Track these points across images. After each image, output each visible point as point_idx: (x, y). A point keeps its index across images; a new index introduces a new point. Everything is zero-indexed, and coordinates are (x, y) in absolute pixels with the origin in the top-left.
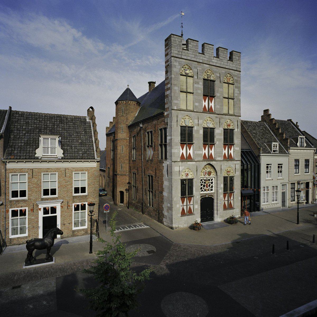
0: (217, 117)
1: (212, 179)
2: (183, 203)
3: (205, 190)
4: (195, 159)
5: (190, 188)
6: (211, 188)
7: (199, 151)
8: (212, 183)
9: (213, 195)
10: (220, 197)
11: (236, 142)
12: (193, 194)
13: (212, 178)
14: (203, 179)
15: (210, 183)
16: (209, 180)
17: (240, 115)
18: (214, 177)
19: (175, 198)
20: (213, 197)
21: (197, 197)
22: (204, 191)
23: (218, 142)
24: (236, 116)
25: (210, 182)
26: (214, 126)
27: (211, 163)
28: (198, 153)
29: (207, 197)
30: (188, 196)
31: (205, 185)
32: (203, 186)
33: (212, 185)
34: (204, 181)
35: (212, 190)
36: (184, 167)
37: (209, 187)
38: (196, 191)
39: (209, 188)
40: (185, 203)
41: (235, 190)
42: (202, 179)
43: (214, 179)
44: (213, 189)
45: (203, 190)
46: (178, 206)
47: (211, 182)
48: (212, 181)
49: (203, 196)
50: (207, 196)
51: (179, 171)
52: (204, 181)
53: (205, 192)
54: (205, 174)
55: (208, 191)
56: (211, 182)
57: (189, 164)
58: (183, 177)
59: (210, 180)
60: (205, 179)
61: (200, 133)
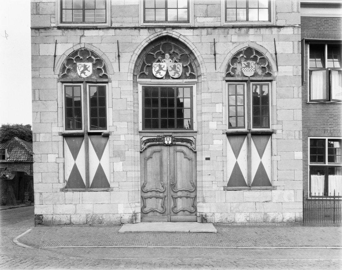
9: (191, 138)
10: (212, 144)
27: (175, 34)
46: (52, 158)
51: (55, 56)
54: (158, 72)
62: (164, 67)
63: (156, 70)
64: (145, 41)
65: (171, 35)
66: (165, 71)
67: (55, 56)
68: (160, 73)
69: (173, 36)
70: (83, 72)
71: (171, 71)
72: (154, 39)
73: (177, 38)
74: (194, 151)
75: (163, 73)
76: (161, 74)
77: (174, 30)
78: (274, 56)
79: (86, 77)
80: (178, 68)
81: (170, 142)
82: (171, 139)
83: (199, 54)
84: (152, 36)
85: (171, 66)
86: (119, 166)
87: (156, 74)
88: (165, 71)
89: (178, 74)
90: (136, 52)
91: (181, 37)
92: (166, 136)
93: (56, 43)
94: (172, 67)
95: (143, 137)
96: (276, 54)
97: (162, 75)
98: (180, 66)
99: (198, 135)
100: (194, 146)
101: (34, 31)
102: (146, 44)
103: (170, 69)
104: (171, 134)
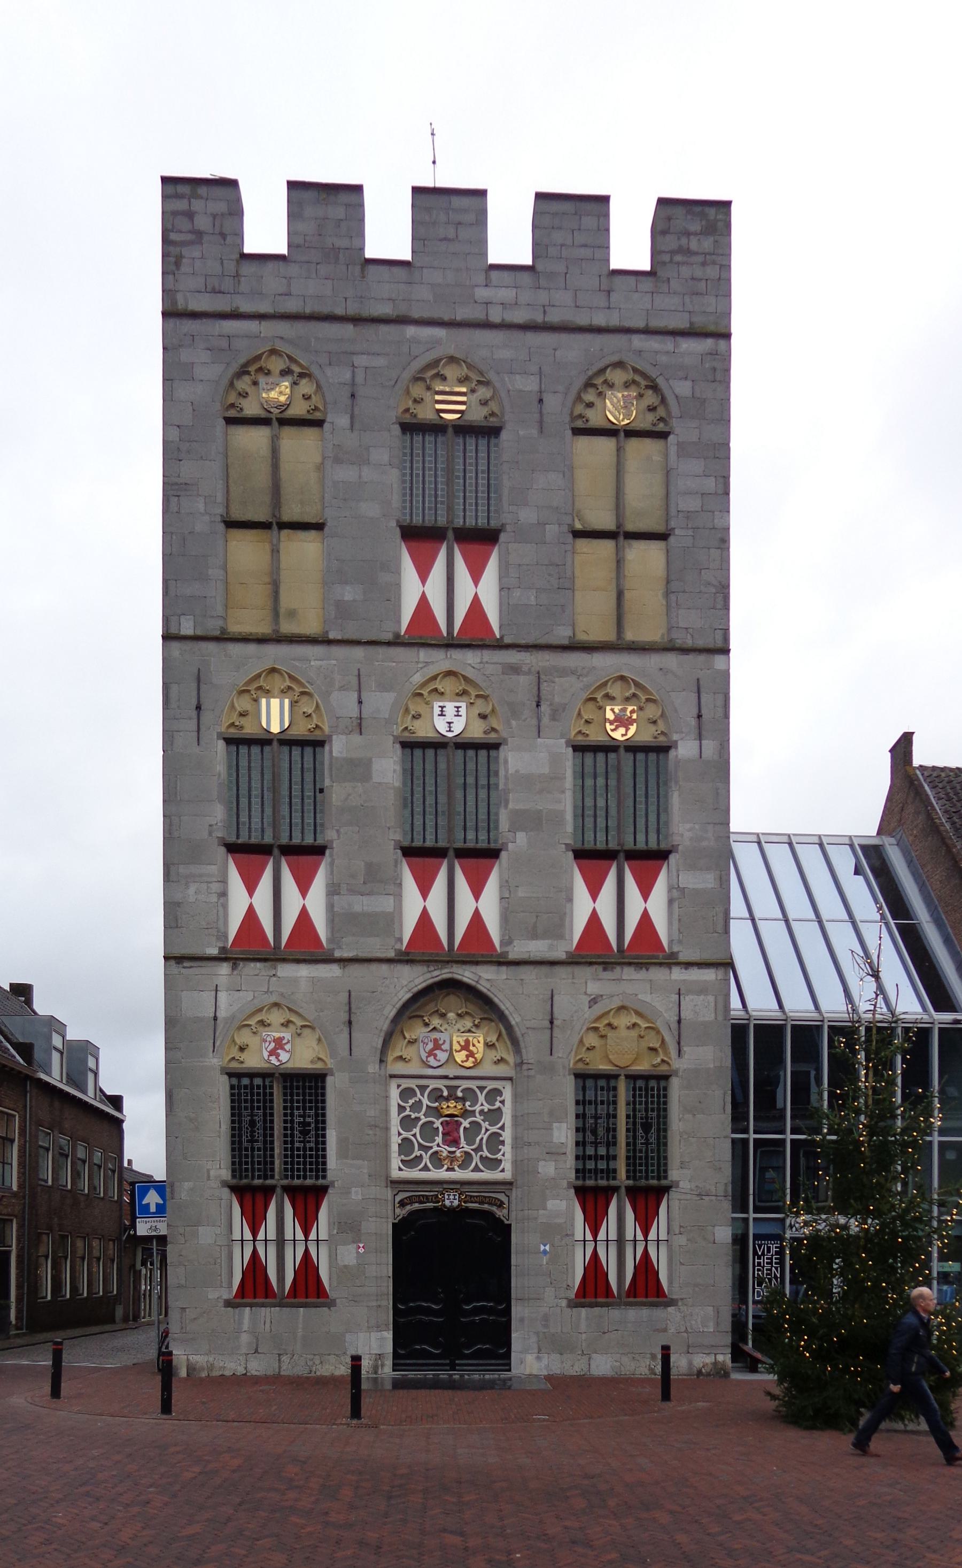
0: (515, 669)
1: (497, 1092)
2: (255, 1221)
3: (437, 1160)
4: (340, 948)
5: (305, 1133)
6: (486, 1153)
7: (370, 894)
8: (494, 1115)
9: (502, 1197)
11: (688, 835)
12: (330, 1174)
13: (491, 1085)
14: (422, 1088)
15: (479, 1119)
16: (469, 1094)
17: (719, 644)
18: (510, 1079)
19: (187, 1185)
20: (500, 1213)
21: (350, 1193)
22: (426, 1168)
23: (521, 837)
24: (685, 651)
25: (478, 1108)
26: (493, 730)
27: (466, 974)
28: (357, 908)
29: (452, 1210)
30: (285, 1182)
31: (438, 1124)
32: (417, 1130)
33: (494, 1129)
34: (425, 1101)
35: (493, 1164)
36: (251, 994)
37: (470, 1142)
38: (343, 1153)
39: (468, 1149)
40: (270, 1227)
41: (674, 1174)
42: (412, 1083)
43: (507, 1094)
44: (499, 1161)
45: (420, 1158)
46: (207, 1235)
47: (482, 1112)
48: (498, 1104)
49: (427, 1199)
50: (451, 1200)
52: (425, 1101)
53: (442, 1174)
54: (431, 1053)
55: (463, 1166)
56: (486, 1107)
57: (295, 981)
58: (243, 1056)
59: (481, 1098)
60: (433, 1084)
61: (376, 778)
62: (443, 1044)
63: (427, 1050)
64: (405, 989)
65: (459, 977)
66: (446, 1051)
67: (215, 1018)
68: (435, 1056)
69: (465, 980)
70: (272, 1053)
71: (459, 1051)
72: (424, 985)
73: (473, 983)
74: (506, 1222)
75: (442, 1056)
76: (438, 1058)
77: (467, 967)
78: (674, 1026)
79: (277, 1064)
80: (474, 1045)
81: (456, 1203)
82: (457, 1197)
83: (518, 1019)
84: (421, 979)
85: (458, 1042)
86: (349, 1255)
87: (427, 1057)
88: (446, 1051)
89: (473, 1057)
90: (386, 1012)
91: (482, 982)
92: (447, 1190)
93: (217, 991)
94: (463, 1044)
95: (399, 1191)
96: (679, 1022)
97: (439, 1061)
98: (479, 1042)
99: (514, 1189)
100: (505, 1211)
101: (173, 962)
102: (409, 995)
103: (456, 1047)
104: (458, 1186)
